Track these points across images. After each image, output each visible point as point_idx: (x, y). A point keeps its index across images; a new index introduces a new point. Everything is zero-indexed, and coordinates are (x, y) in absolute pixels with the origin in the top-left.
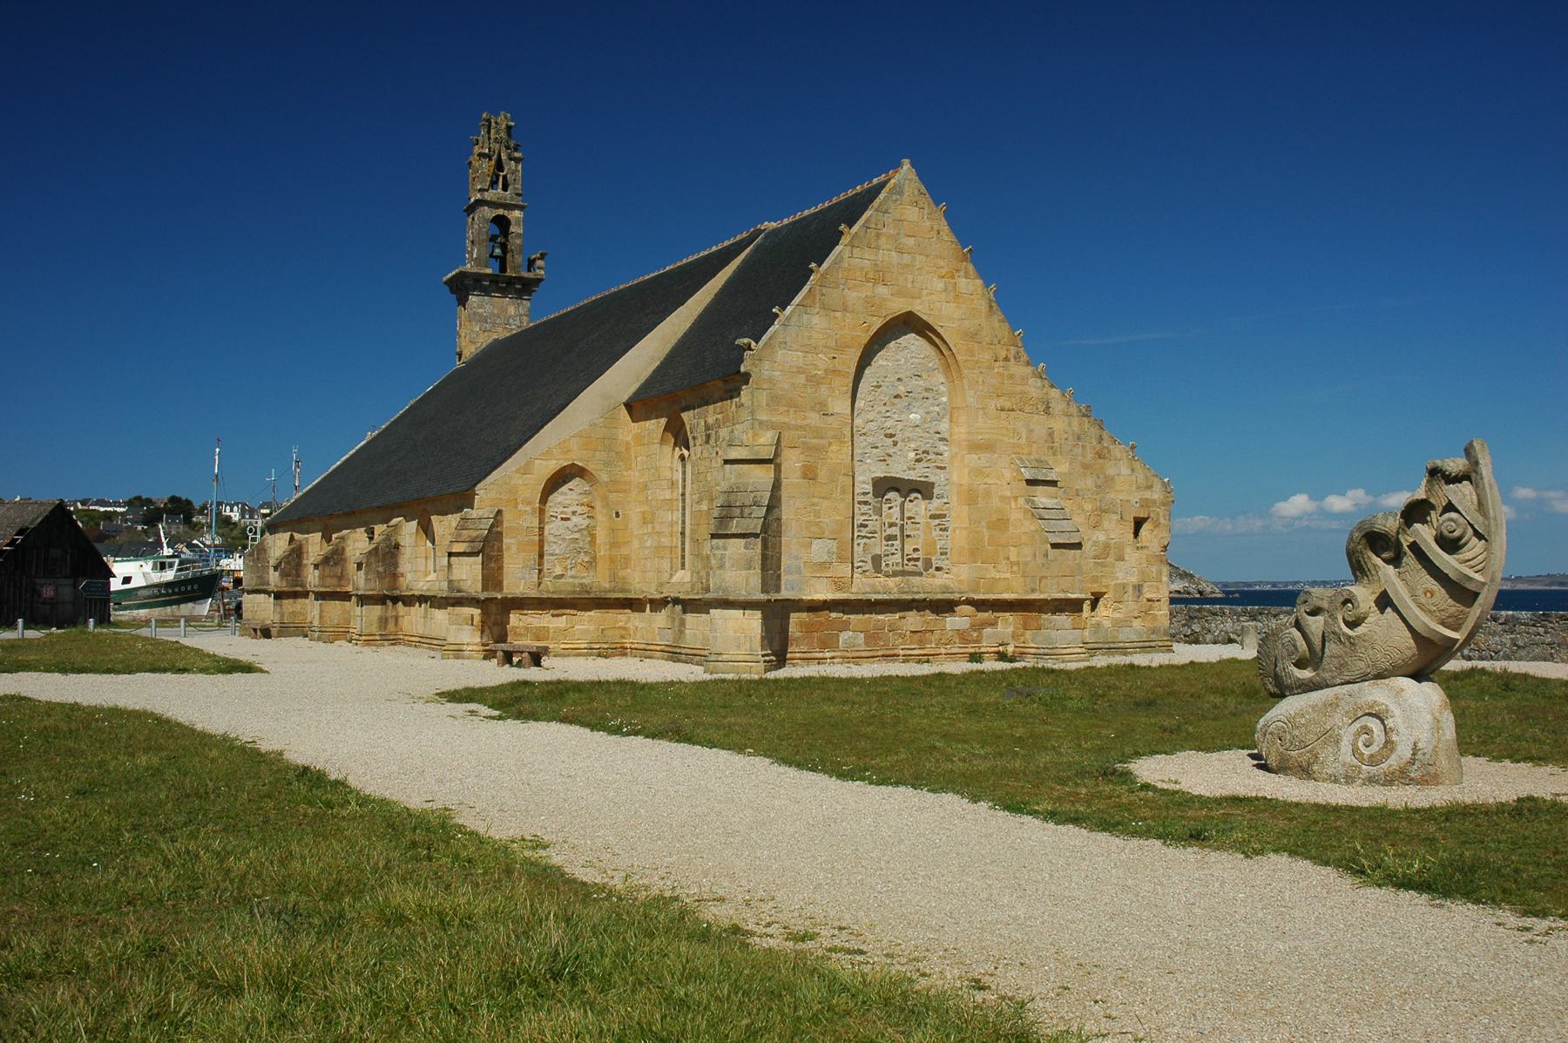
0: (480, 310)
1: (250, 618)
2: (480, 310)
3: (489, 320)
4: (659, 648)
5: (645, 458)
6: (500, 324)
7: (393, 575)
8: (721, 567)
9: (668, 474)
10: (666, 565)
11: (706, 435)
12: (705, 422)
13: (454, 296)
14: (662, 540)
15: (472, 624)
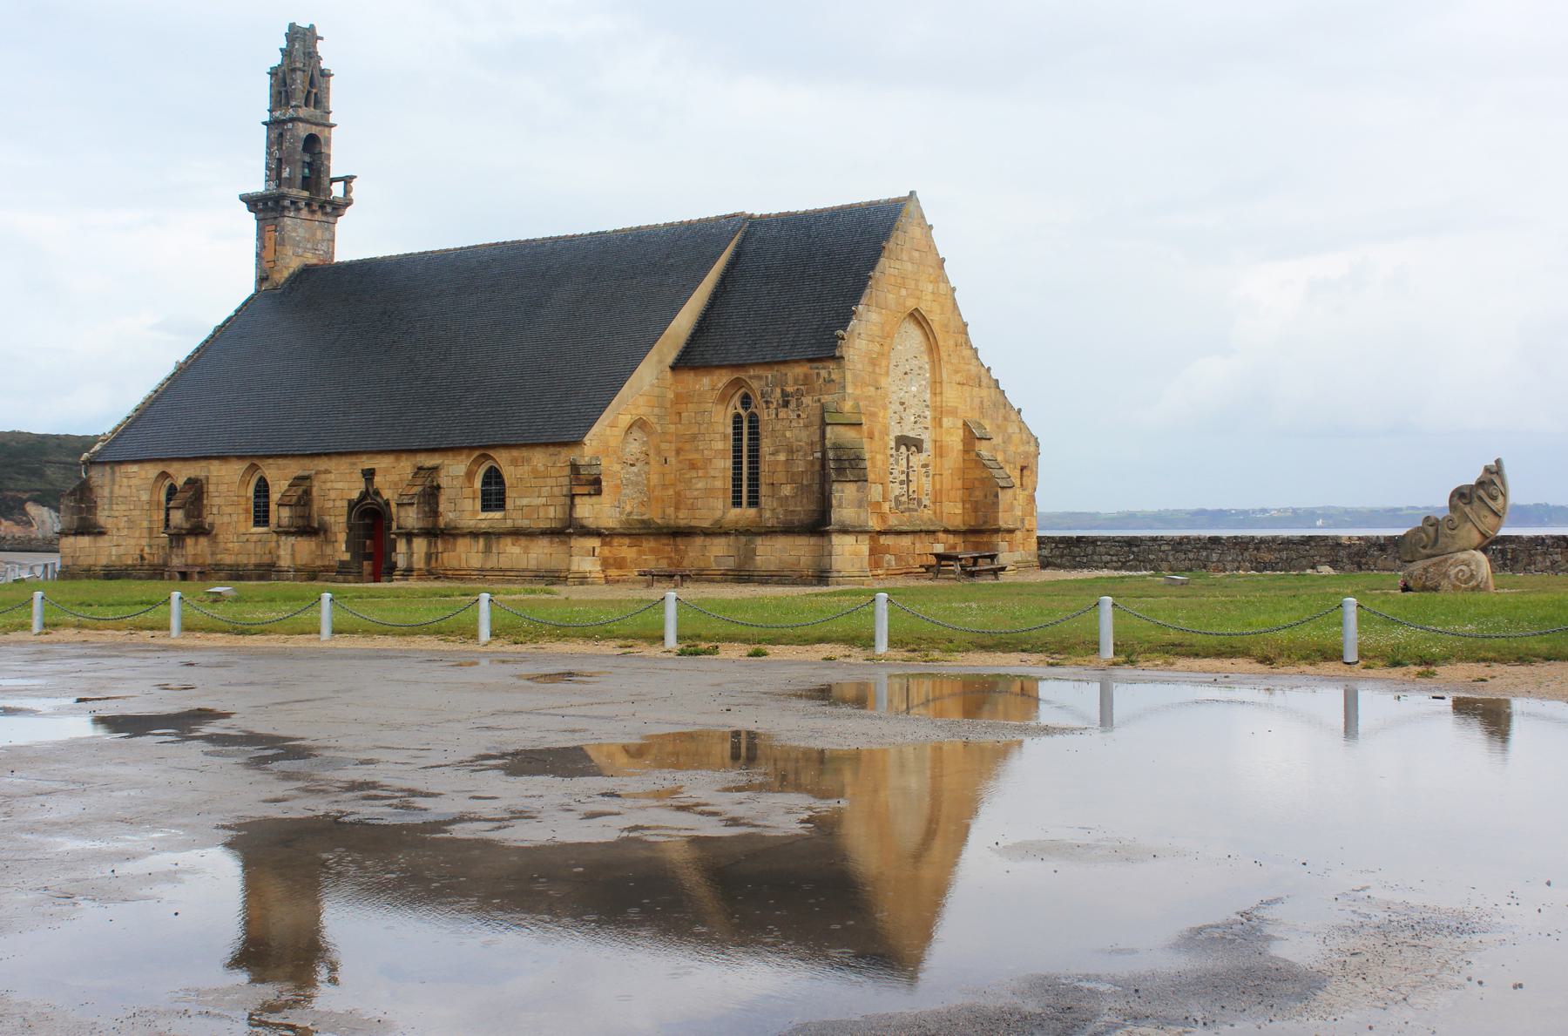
0: (294, 234)
1: (70, 563)
2: (294, 234)
3: (301, 245)
4: (719, 572)
5: (693, 414)
6: (309, 249)
7: (435, 513)
8: (840, 506)
9: (721, 429)
10: (719, 504)
11: (784, 400)
12: (783, 390)
13: (253, 214)
14: (716, 483)
15: (594, 556)
